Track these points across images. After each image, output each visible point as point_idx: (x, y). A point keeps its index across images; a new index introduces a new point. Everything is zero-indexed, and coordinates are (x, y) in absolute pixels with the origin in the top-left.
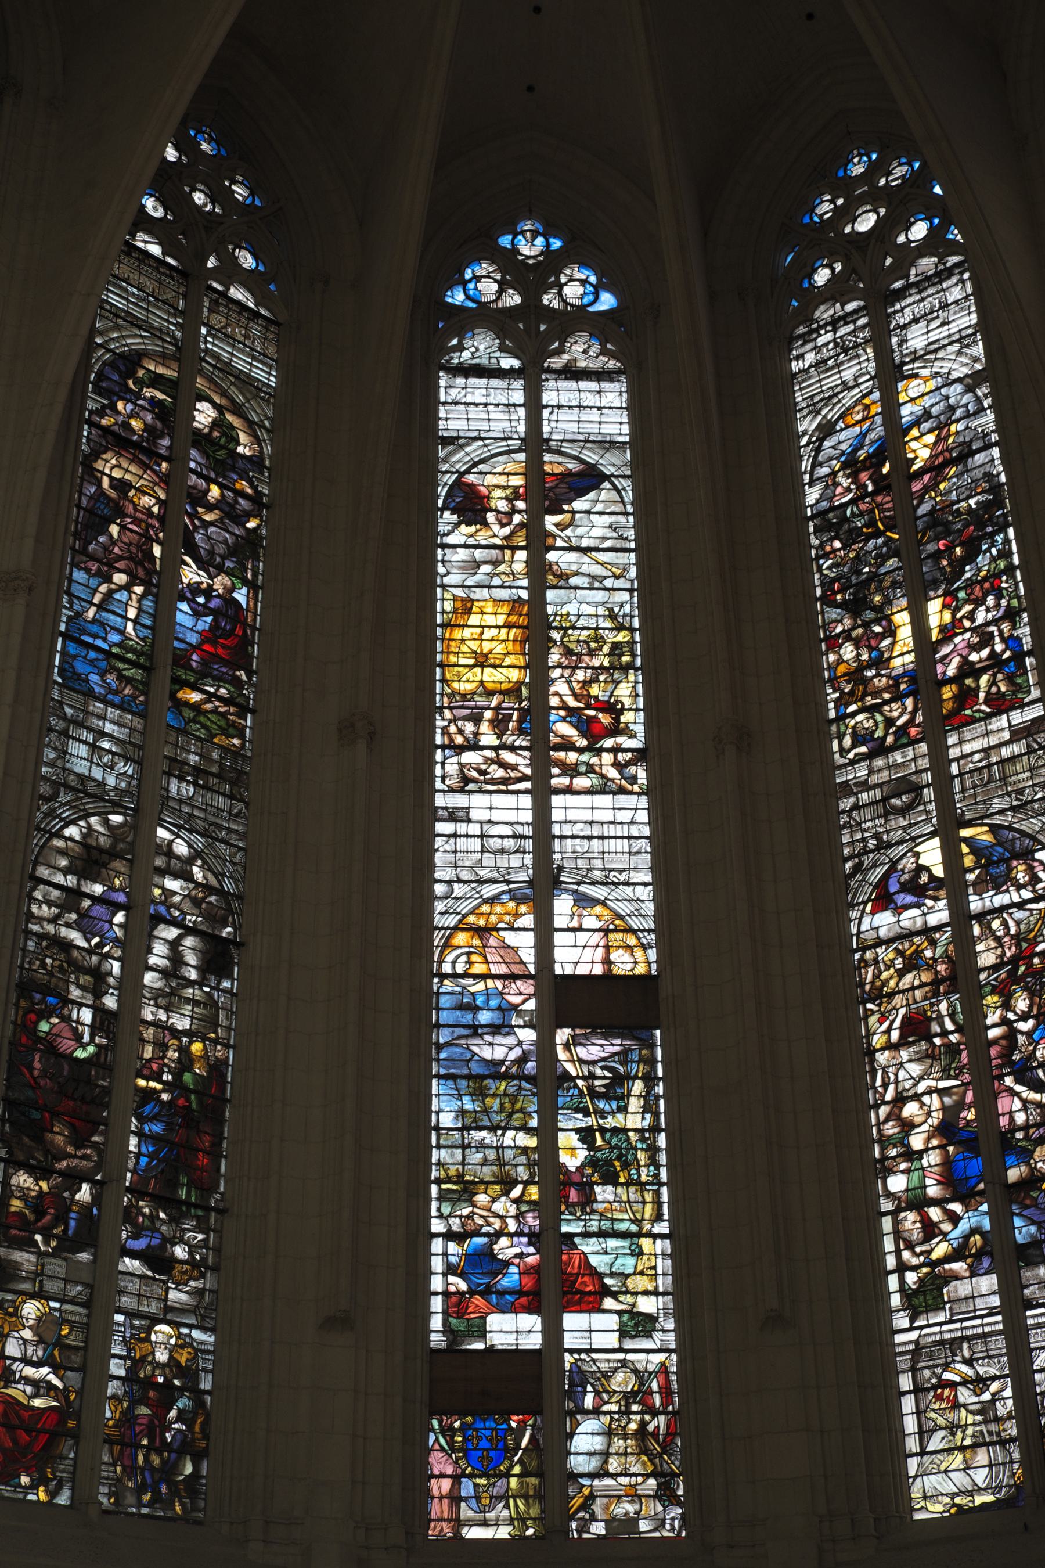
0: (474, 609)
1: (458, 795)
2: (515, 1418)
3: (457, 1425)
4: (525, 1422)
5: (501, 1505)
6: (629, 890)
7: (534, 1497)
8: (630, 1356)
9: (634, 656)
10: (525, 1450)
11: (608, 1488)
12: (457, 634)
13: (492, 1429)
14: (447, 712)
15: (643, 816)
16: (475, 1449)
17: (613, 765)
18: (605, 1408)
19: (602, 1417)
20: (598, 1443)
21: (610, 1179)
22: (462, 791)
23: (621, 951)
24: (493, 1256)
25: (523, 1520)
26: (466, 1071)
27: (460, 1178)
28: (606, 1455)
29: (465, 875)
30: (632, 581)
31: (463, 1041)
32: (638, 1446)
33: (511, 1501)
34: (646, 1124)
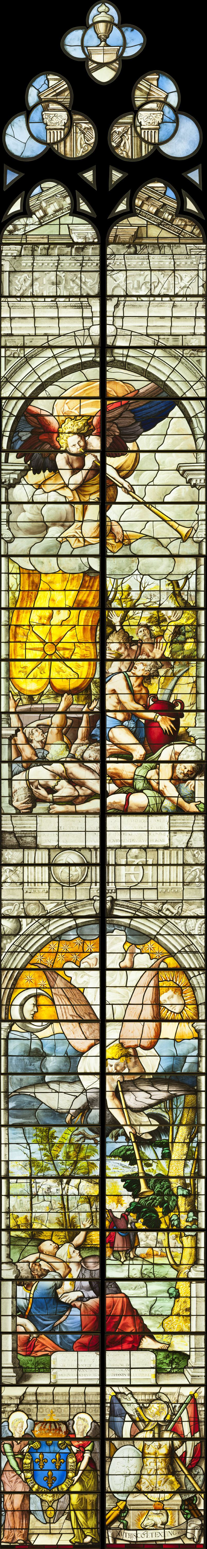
0: (42, 586)
1: (25, 817)
3: (26, 1449)
6: (180, 923)
8: (164, 1390)
9: (197, 642)
12: (24, 618)
14: (13, 717)
15: (199, 840)
17: (171, 779)
21: (153, 1226)
22: (30, 812)
23: (170, 992)
24: (56, 1299)
26: (33, 1121)
29: (33, 910)
30: (200, 543)
31: (31, 1090)
32: (167, 1468)
34: (188, 1171)
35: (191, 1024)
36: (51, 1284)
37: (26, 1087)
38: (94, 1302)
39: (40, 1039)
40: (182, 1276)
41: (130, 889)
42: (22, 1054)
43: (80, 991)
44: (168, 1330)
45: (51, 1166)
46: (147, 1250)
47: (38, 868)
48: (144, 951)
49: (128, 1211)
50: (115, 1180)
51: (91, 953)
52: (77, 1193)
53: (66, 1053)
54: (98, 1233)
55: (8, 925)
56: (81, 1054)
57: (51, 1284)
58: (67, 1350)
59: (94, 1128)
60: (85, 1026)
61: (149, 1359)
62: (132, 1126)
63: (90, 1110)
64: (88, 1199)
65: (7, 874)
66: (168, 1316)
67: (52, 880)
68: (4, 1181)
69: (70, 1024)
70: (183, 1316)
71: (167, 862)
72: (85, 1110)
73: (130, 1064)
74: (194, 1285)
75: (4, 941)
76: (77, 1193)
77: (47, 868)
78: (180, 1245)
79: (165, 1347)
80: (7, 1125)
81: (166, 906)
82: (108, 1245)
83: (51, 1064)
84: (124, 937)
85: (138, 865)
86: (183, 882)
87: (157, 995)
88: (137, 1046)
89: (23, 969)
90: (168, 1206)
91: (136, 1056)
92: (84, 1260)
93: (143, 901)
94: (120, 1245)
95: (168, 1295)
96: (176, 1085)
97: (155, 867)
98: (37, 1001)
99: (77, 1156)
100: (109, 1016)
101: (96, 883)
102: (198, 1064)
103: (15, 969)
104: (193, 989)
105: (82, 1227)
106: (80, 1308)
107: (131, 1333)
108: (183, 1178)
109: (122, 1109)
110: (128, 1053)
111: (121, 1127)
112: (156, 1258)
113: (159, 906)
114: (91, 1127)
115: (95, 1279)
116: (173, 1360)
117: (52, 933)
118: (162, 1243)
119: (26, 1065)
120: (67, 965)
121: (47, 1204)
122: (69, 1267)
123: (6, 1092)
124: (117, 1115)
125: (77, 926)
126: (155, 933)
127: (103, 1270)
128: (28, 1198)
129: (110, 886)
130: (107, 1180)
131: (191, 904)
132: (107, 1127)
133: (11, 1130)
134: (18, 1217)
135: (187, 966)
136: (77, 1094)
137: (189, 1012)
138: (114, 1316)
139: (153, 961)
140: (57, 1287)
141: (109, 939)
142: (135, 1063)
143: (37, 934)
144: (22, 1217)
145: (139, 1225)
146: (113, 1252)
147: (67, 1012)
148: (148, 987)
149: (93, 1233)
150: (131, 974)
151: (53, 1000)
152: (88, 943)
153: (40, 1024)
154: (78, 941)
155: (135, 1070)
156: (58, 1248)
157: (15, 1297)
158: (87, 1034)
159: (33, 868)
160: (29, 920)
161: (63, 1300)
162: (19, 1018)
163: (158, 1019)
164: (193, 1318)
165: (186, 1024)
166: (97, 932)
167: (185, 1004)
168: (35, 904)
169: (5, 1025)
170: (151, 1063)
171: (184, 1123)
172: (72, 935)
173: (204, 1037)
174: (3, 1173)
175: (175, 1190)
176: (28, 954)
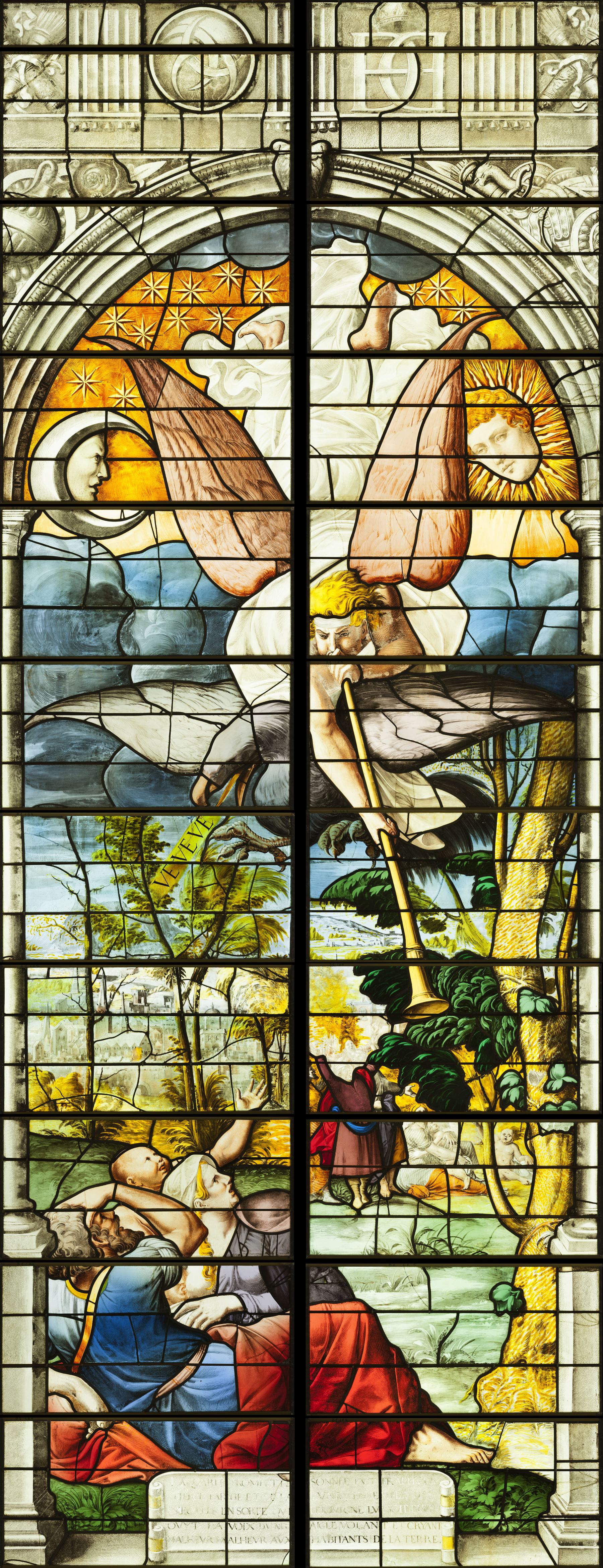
6: (528, 221)
21: (448, 1104)
23: (498, 422)
26: (96, 797)
27: (83, 1108)
29: (96, 181)
31: (90, 706)
34: (549, 944)
35: (557, 514)
36: (148, 1273)
37: (74, 699)
38: (272, 1327)
39: (116, 559)
40: (531, 1250)
41: (380, 120)
42: (64, 600)
43: (234, 420)
44: (490, 1407)
45: (146, 929)
46: (429, 1175)
47: (111, 61)
48: (421, 301)
49: (375, 1061)
50: (336, 969)
51: (266, 306)
52: (224, 1008)
53: (193, 598)
54: (287, 1124)
55: (21, 224)
56: (236, 602)
57: (148, 1273)
58: (194, 1468)
59: (276, 818)
60: (247, 520)
61: (436, 1493)
62: (385, 811)
63: (262, 767)
64: (259, 1025)
65: (21, 75)
66: (492, 1367)
67: (152, 94)
68: (10, 973)
69: (204, 514)
70: (535, 1366)
71: (488, 40)
72: (248, 765)
73: (381, 631)
74: (567, 1276)
75: (12, 273)
76: (224, 1008)
77: (136, 59)
78: (526, 1159)
79: (482, 1457)
80: (20, 811)
81: (485, 170)
82: (316, 1160)
83: (148, 632)
84: (364, 261)
85: (402, 49)
86: (536, 100)
87: (460, 428)
88: (400, 579)
89: (68, 352)
90: (490, 1047)
91: (398, 607)
92: (244, 1203)
93: (418, 156)
94: (352, 1160)
95: (490, 1306)
96: (513, 693)
97: (454, 56)
98: (106, 446)
99: (225, 901)
100: (317, 490)
101: (280, 101)
102: (579, 630)
103: (43, 354)
104: (566, 411)
105: (240, 1107)
106: (232, 1344)
107: (383, 1415)
108: (536, 963)
109: (356, 762)
110: (375, 598)
111: (354, 814)
112: (456, 1198)
113: (464, 168)
114: (265, 814)
115: (278, 1260)
116: (507, 1495)
117: (151, 249)
118: (473, 1154)
119: (75, 633)
120: (194, 344)
121: (135, 1039)
122: (200, 1224)
123: (18, 711)
124: (342, 778)
125: (225, 229)
126: (452, 249)
127: (300, 1233)
128: (81, 1024)
129: (323, 113)
130: (313, 970)
131: (557, 165)
132: (314, 816)
133: (32, 825)
134: (51, 1077)
135: (547, 345)
136: (225, 720)
137: (554, 479)
138: (334, 1366)
139: (448, 330)
140: (164, 1283)
141: (318, 266)
142: (396, 627)
143: (108, 253)
144: (63, 1077)
145: (407, 1100)
146: (331, 1180)
147: (192, 479)
148: (432, 405)
149: (272, 1124)
150: (385, 368)
151: (153, 443)
152: (257, 277)
153: (115, 514)
154: (228, 271)
155: (394, 649)
156: (169, 1169)
157: (41, 1312)
158: (255, 544)
159: (95, 57)
160: (84, 211)
161: (185, 1320)
162: (55, 497)
163: (462, 500)
164: (566, 1374)
165: (544, 514)
166: (283, 246)
167: (540, 457)
168: (102, 163)
169: (13, 517)
170: (441, 629)
171: (538, 802)
172: (210, 254)
173: (596, 552)
174: (8, 950)
175: (512, 999)
176: (80, 311)
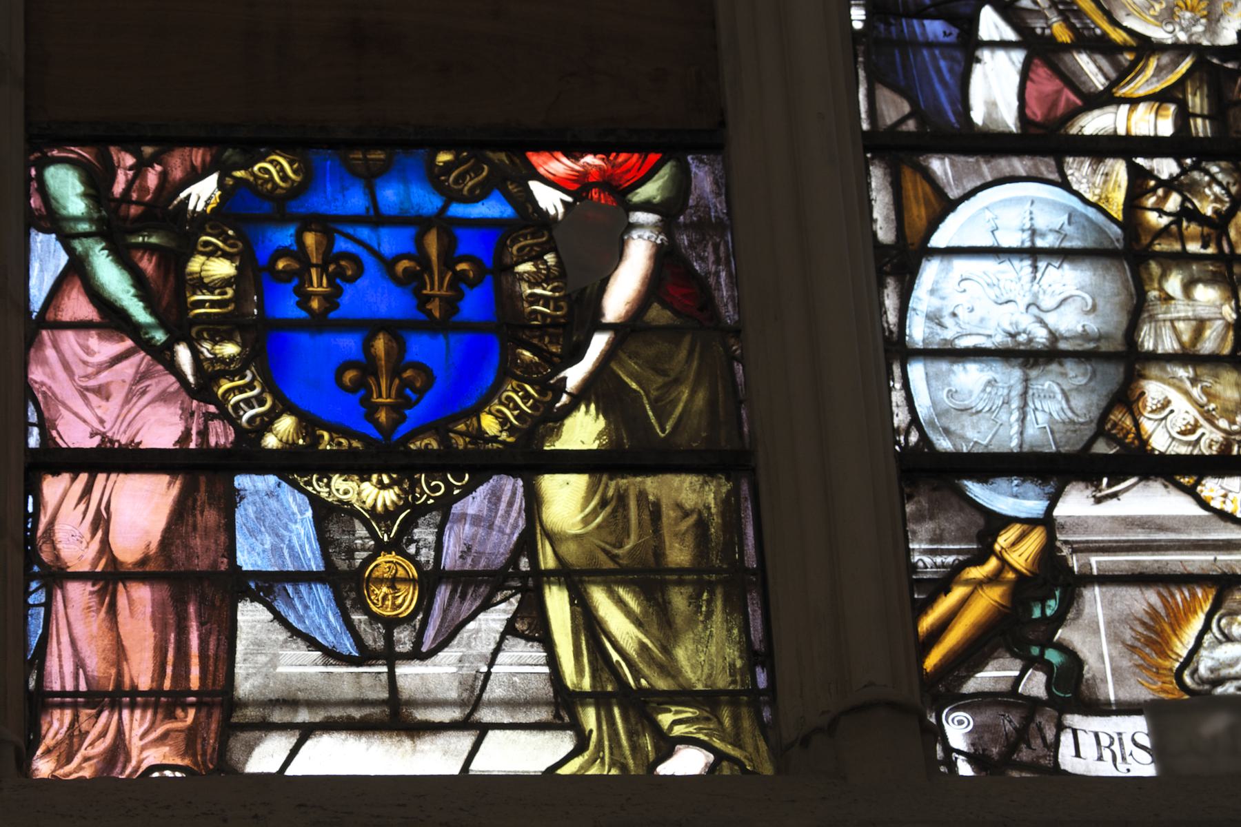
2: (559, 166)
4: (618, 191)
5: (493, 620)
7: (698, 578)
10: (624, 331)
11: (1150, 534)
13: (421, 223)
16: (320, 323)
18: (1094, 123)
19: (1079, 171)
20: (1071, 301)
25: (640, 706)
28: (1122, 363)
33: (557, 602)
